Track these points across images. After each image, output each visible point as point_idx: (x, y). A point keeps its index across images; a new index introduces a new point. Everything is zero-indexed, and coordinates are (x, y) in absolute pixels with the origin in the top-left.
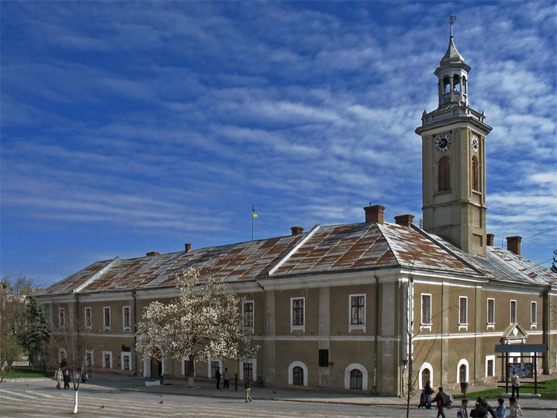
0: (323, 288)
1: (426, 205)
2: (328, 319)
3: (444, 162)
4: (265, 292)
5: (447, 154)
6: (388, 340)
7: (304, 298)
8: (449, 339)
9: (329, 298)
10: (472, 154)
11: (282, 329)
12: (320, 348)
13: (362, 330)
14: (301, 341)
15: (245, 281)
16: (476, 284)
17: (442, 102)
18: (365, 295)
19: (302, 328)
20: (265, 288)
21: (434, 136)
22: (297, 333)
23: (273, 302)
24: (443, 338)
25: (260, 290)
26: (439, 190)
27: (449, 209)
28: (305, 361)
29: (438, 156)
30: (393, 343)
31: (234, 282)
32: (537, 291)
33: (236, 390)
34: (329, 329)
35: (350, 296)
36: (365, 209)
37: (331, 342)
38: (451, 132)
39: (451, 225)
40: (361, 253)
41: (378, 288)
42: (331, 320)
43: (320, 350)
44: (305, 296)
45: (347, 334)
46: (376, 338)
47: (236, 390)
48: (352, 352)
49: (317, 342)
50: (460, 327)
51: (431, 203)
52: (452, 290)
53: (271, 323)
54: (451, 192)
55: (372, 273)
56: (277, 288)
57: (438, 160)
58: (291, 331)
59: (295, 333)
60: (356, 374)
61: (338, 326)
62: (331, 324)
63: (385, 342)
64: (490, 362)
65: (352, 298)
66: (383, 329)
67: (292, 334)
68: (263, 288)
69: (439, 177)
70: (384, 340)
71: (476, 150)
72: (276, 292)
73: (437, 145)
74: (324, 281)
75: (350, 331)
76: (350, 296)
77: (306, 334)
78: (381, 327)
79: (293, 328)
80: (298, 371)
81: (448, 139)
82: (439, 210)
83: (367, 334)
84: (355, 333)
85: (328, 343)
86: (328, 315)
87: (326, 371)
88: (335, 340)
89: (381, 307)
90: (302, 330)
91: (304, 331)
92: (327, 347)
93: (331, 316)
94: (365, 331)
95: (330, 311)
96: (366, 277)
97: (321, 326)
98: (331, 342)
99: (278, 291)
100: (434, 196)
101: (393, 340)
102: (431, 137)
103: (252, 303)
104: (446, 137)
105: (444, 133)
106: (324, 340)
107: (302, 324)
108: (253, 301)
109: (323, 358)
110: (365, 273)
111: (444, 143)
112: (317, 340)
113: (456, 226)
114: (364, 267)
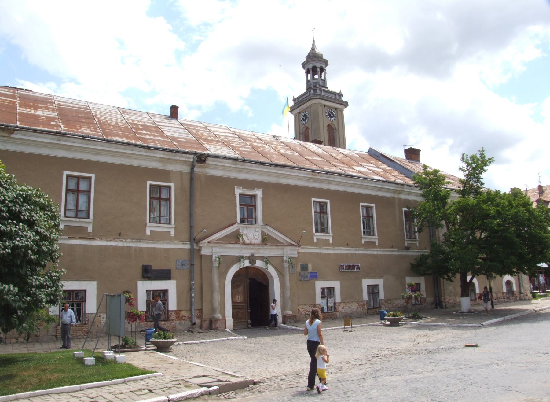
5: (335, 123)
29: (329, 123)
38: (336, 109)
81: (334, 113)
104: (332, 111)
105: (332, 108)
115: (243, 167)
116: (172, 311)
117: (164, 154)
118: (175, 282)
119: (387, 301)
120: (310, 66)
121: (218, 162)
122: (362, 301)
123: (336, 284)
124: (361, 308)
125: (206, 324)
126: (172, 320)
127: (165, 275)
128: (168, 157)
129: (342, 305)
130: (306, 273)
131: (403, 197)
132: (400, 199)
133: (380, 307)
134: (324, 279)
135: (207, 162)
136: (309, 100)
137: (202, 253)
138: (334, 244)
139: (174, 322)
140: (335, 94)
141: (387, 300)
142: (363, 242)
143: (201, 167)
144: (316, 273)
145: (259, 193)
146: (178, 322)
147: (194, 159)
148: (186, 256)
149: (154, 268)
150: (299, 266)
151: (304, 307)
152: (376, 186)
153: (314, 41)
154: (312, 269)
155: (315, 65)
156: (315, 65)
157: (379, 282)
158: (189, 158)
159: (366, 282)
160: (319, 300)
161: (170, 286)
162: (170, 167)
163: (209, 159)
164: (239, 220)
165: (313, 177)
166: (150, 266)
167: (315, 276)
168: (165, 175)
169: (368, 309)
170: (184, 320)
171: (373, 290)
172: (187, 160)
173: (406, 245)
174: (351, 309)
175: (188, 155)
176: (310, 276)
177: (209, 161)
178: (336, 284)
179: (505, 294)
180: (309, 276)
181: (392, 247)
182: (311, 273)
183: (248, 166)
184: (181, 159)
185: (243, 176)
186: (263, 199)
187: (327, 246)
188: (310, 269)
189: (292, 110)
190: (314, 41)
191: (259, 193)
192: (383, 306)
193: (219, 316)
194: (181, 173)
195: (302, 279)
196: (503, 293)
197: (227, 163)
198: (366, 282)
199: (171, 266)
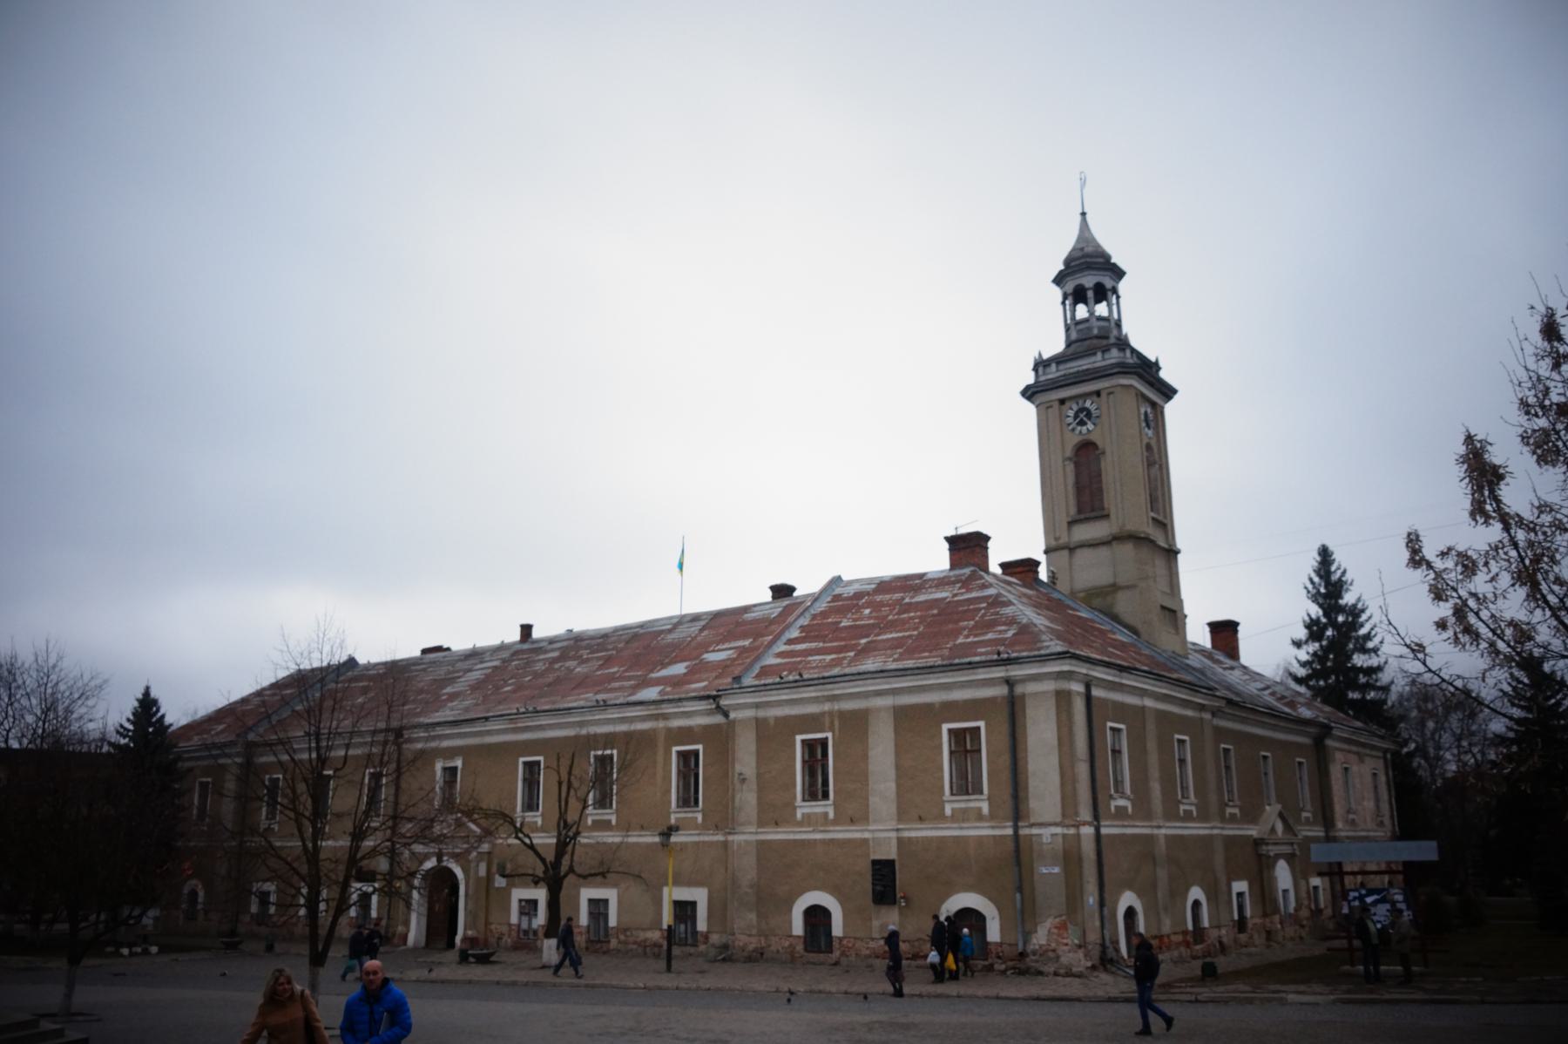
0: (879, 710)
1: (1053, 543)
2: (892, 785)
3: (1086, 452)
4: (734, 721)
5: (1094, 437)
7: (829, 735)
8: (1166, 836)
9: (891, 729)
10: (1145, 441)
11: (774, 812)
13: (980, 809)
14: (823, 841)
15: (680, 700)
16: (1202, 708)
17: (1074, 336)
18: (981, 724)
19: (826, 808)
20: (732, 715)
21: (1062, 402)
22: (812, 822)
23: (753, 748)
24: (1156, 831)
25: (718, 719)
26: (1080, 511)
27: (1104, 552)
28: (835, 891)
29: (1073, 440)
31: (654, 702)
32: (1306, 734)
33: (669, 969)
34: (893, 809)
35: (945, 727)
36: (948, 539)
37: (900, 840)
38: (1098, 393)
39: (1114, 588)
40: (957, 633)
41: (1013, 708)
42: (899, 786)
43: (875, 862)
44: (832, 729)
45: (941, 817)
46: (1016, 828)
47: (669, 969)
48: (954, 864)
49: (866, 841)
50: (1182, 808)
51: (1064, 540)
52: (1162, 716)
53: (747, 799)
54: (1107, 516)
55: (999, 673)
56: (761, 713)
57: (1069, 452)
58: (799, 816)
59: (808, 820)
61: (914, 800)
62: (899, 795)
63: (1040, 835)
64: (1240, 895)
65: (950, 731)
66: (1033, 804)
67: (800, 824)
68: (726, 715)
69: (1079, 488)
70: (1035, 831)
71: (1150, 433)
72: (760, 724)
73: (1070, 420)
75: (948, 811)
76: (945, 727)
77: (835, 822)
78: (1027, 798)
79: (804, 809)
80: (817, 916)
81: (1093, 408)
82: (1083, 556)
84: (961, 816)
85: (894, 843)
86: (892, 773)
88: (913, 834)
89: (1026, 750)
90: (826, 814)
91: (831, 815)
92: (892, 854)
95: (898, 767)
97: (874, 800)
99: (765, 720)
100: (1071, 524)
101: (1058, 830)
102: (1056, 404)
103: (696, 753)
104: (1088, 404)
106: (882, 833)
107: (826, 796)
108: (700, 747)
109: (884, 881)
110: (982, 674)
111: (1083, 416)
112: (867, 835)
113: (1128, 587)
114: (977, 659)
119: (622, 929)
131: (676, 723)
132: (669, 730)
141: (625, 930)
145: (459, 763)
153: (1083, 214)
155: (1089, 274)
156: (1089, 274)
160: (514, 919)
173: (673, 821)
181: (642, 828)
183: (439, 731)
190: (1083, 214)
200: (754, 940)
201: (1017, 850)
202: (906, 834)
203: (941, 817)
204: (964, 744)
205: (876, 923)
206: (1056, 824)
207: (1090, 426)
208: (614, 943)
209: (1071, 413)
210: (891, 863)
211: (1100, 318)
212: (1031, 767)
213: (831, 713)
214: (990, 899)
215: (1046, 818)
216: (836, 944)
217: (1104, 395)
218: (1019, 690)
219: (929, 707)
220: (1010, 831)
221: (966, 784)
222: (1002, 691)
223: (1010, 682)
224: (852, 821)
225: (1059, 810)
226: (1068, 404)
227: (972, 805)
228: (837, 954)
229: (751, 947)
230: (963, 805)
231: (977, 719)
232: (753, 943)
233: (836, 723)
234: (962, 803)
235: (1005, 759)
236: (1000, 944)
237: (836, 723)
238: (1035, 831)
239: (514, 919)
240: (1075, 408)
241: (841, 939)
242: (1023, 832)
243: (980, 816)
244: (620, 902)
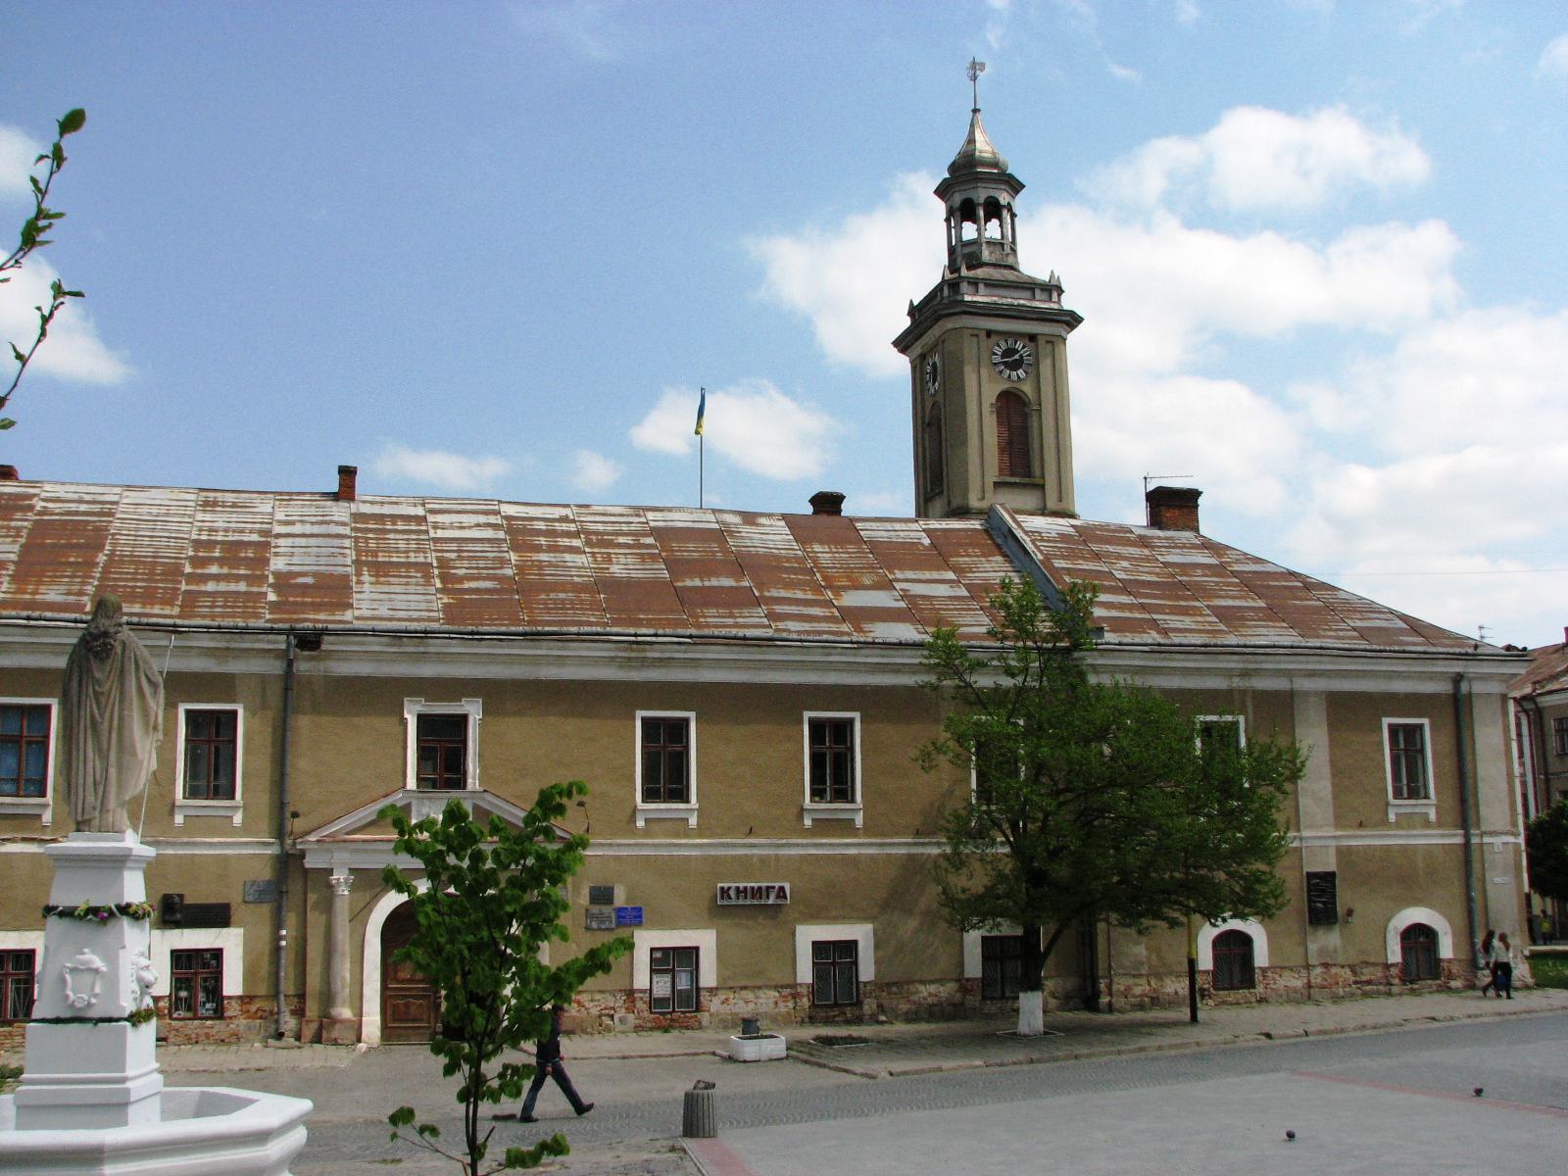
0: (1307, 694)
5: (1027, 388)
6: (1497, 841)
12: (1306, 869)
18: (1425, 721)
21: (989, 333)
30: (1511, 847)
34: (1330, 811)
37: (1339, 850)
38: (1033, 338)
43: (1309, 875)
45: (1384, 822)
46: (1467, 836)
55: (1457, 667)
57: (994, 401)
60: (1419, 938)
62: (1335, 797)
65: (1390, 726)
74: (1312, 674)
75: (1392, 817)
76: (1386, 721)
78: (1477, 805)
81: (1025, 352)
83: (1439, 824)
84: (1406, 822)
85: (1332, 852)
87: (1329, 939)
88: (1353, 843)
92: (1327, 863)
93: (1334, 775)
94: (1433, 816)
96: (1432, 677)
98: (1339, 850)
104: (1019, 345)
115: (422, 649)
116: (230, 998)
117: (211, 640)
118: (241, 931)
119: (882, 985)
120: (957, 199)
121: (352, 645)
122: (794, 986)
123: (705, 940)
124: (791, 1004)
125: (309, 1031)
126: (231, 1018)
127: (216, 916)
128: (223, 645)
129: (722, 996)
130: (606, 909)
133: (859, 1004)
134: (666, 922)
135: (323, 647)
136: (937, 320)
137: (307, 866)
138: (700, 831)
139: (236, 1022)
140: (1031, 286)
142: (808, 822)
143: (312, 659)
144: (640, 909)
146: (245, 1022)
147: (289, 643)
148: (266, 873)
149: (189, 900)
150: (586, 892)
151: (598, 996)
152: (858, 660)
154: (628, 899)
157: (861, 933)
158: (275, 642)
159: (809, 934)
160: (642, 979)
161: (231, 942)
162: (234, 667)
163: (326, 638)
164: (411, 783)
165: (633, 654)
166: (181, 896)
167: (633, 917)
168: (222, 684)
169: (813, 1006)
170: (261, 1018)
171: (835, 957)
172: (271, 647)
174: (751, 1006)
175: (271, 637)
176: (619, 917)
177: (328, 644)
178: (705, 940)
179: (1394, 971)
180: (613, 915)
182: (620, 910)
184: (257, 646)
185: (428, 670)
186: (483, 724)
187: (677, 835)
188: (620, 898)
189: (903, 343)
190: (975, 111)
191: (473, 710)
192: (867, 1001)
193: (345, 1012)
194: (263, 679)
195: (594, 925)
196: (1387, 966)
197: (375, 645)
198: (809, 934)
199: (233, 895)
200: (1143, 981)
201: (1467, 862)
202: (1345, 843)
203: (1384, 822)
204: (1407, 743)
205: (1313, 947)
206: (1506, 833)
207: (1021, 372)
208: (869, 1006)
209: (999, 351)
210: (1329, 877)
211: (991, 243)
212: (1481, 772)
213: (1243, 692)
214: (1442, 913)
215: (1499, 827)
216: (1258, 976)
217: (1041, 342)
218: (1464, 687)
219: (1368, 697)
220: (1459, 840)
221: (1411, 785)
222: (1444, 688)
223: (1458, 679)
224: (1361, 825)
225: (1508, 819)
226: (994, 339)
227: (1417, 810)
228: (1260, 989)
229: (1138, 991)
230: (1409, 810)
231: (1420, 716)
232: (1140, 988)
233: (1249, 703)
234: (1408, 805)
235: (1449, 764)
236: (1449, 961)
237: (1249, 703)
238: (1486, 840)
239: (642, 979)
240: (1004, 346)
241: (1264, 970)
242: (1475, 840)
243: (1427, 824)
244: (878, 945)
